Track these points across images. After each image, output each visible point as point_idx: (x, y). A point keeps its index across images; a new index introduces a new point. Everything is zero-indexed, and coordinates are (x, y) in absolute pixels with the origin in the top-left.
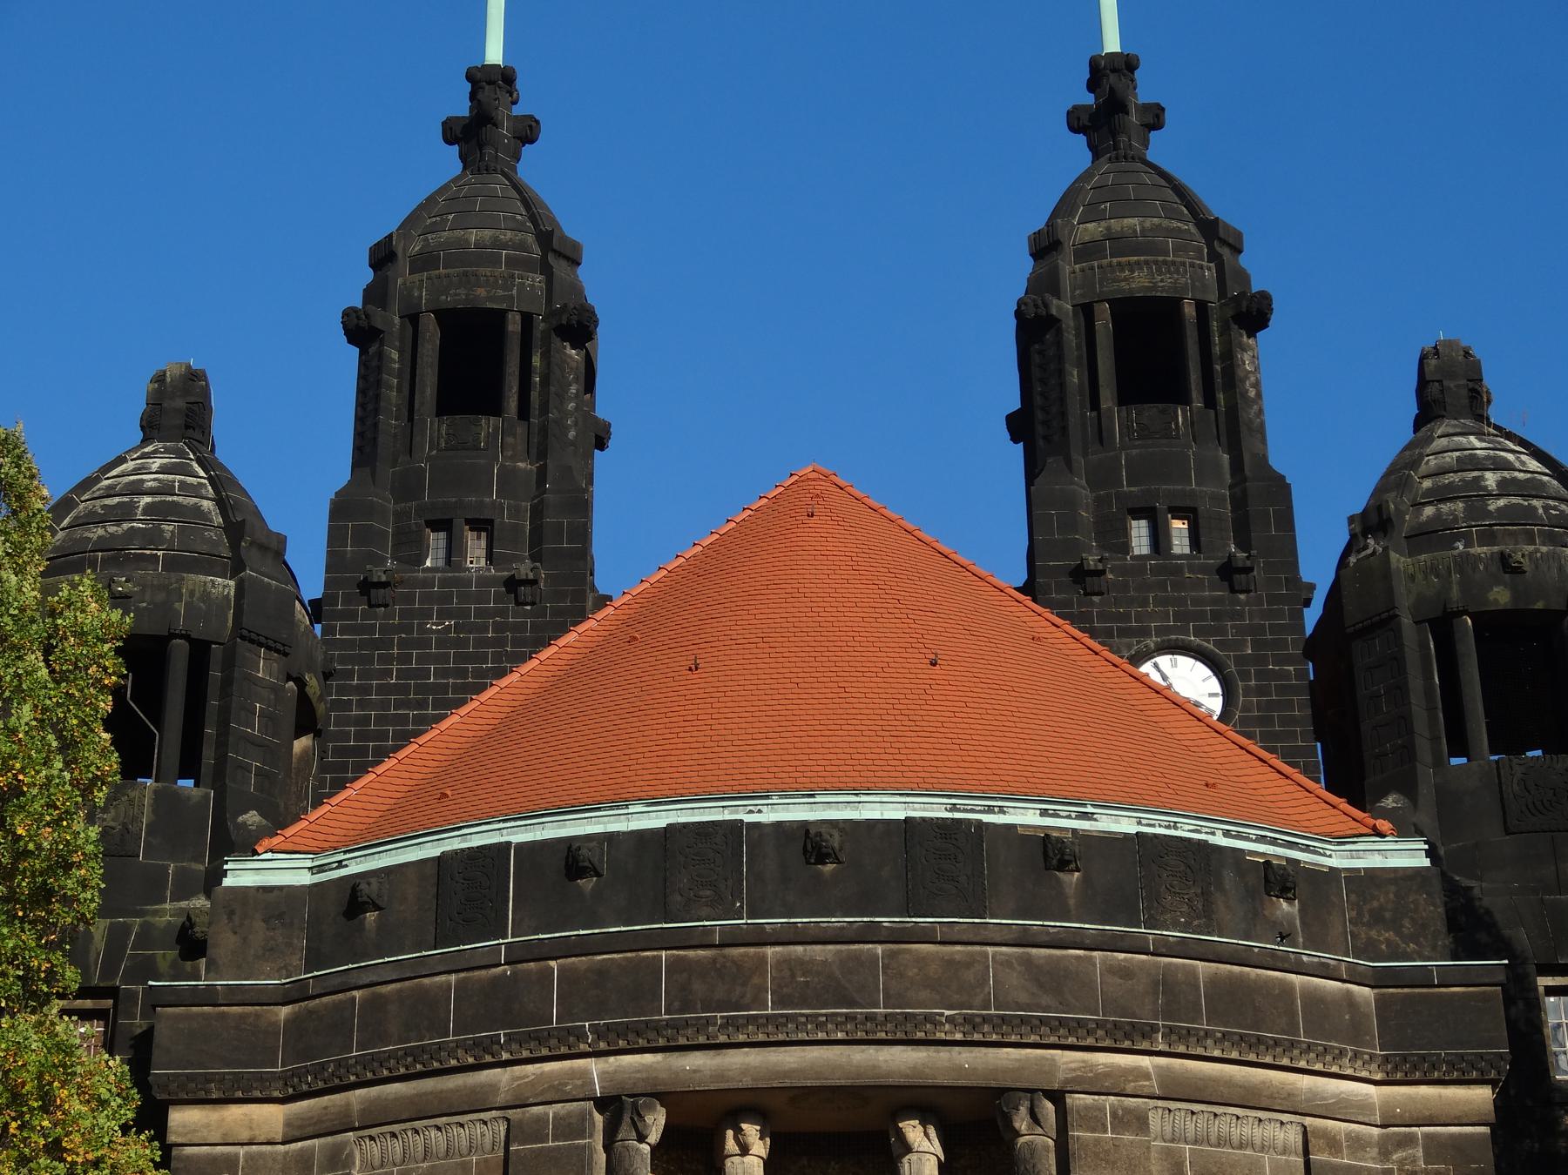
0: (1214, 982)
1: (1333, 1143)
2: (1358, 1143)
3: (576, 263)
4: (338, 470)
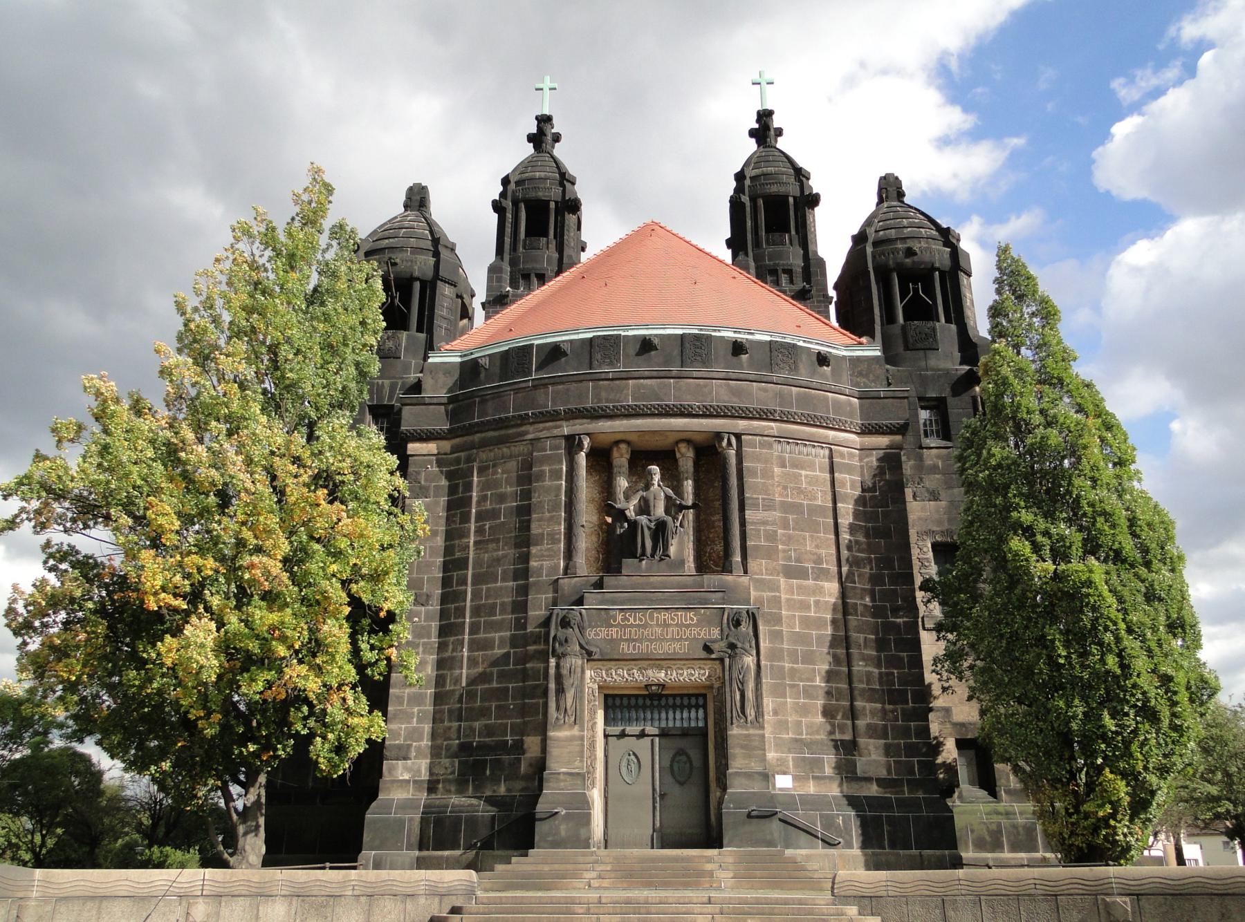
0: (798, 394)
1: (842, 455)
2: (851, 456)
3: (573, 184)
4: (491, 257)
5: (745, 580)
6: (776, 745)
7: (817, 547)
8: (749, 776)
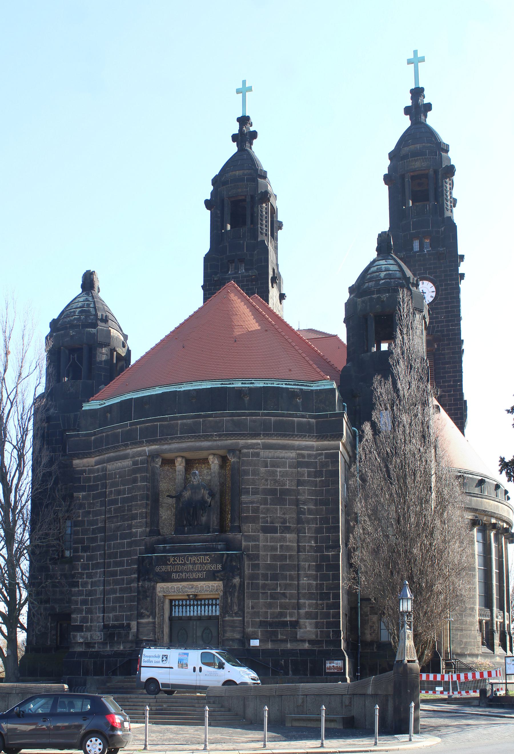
5: (239, 536)
6: (252, 624)
7: (284, 514)
8: (233, 640)
